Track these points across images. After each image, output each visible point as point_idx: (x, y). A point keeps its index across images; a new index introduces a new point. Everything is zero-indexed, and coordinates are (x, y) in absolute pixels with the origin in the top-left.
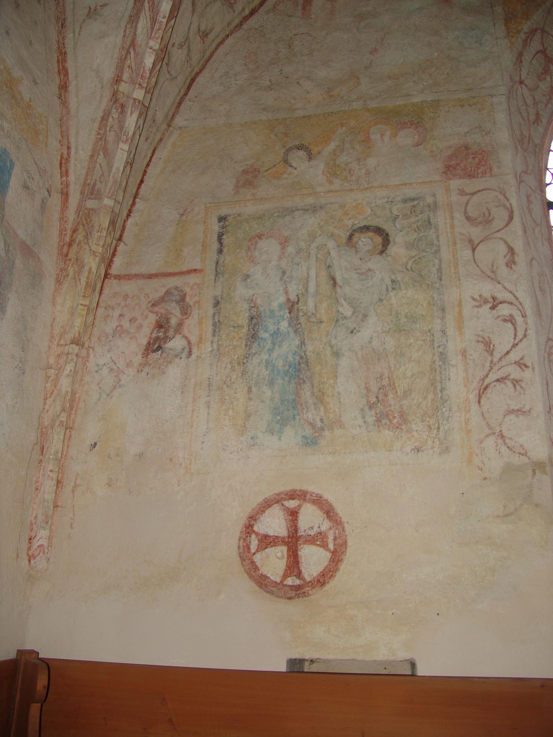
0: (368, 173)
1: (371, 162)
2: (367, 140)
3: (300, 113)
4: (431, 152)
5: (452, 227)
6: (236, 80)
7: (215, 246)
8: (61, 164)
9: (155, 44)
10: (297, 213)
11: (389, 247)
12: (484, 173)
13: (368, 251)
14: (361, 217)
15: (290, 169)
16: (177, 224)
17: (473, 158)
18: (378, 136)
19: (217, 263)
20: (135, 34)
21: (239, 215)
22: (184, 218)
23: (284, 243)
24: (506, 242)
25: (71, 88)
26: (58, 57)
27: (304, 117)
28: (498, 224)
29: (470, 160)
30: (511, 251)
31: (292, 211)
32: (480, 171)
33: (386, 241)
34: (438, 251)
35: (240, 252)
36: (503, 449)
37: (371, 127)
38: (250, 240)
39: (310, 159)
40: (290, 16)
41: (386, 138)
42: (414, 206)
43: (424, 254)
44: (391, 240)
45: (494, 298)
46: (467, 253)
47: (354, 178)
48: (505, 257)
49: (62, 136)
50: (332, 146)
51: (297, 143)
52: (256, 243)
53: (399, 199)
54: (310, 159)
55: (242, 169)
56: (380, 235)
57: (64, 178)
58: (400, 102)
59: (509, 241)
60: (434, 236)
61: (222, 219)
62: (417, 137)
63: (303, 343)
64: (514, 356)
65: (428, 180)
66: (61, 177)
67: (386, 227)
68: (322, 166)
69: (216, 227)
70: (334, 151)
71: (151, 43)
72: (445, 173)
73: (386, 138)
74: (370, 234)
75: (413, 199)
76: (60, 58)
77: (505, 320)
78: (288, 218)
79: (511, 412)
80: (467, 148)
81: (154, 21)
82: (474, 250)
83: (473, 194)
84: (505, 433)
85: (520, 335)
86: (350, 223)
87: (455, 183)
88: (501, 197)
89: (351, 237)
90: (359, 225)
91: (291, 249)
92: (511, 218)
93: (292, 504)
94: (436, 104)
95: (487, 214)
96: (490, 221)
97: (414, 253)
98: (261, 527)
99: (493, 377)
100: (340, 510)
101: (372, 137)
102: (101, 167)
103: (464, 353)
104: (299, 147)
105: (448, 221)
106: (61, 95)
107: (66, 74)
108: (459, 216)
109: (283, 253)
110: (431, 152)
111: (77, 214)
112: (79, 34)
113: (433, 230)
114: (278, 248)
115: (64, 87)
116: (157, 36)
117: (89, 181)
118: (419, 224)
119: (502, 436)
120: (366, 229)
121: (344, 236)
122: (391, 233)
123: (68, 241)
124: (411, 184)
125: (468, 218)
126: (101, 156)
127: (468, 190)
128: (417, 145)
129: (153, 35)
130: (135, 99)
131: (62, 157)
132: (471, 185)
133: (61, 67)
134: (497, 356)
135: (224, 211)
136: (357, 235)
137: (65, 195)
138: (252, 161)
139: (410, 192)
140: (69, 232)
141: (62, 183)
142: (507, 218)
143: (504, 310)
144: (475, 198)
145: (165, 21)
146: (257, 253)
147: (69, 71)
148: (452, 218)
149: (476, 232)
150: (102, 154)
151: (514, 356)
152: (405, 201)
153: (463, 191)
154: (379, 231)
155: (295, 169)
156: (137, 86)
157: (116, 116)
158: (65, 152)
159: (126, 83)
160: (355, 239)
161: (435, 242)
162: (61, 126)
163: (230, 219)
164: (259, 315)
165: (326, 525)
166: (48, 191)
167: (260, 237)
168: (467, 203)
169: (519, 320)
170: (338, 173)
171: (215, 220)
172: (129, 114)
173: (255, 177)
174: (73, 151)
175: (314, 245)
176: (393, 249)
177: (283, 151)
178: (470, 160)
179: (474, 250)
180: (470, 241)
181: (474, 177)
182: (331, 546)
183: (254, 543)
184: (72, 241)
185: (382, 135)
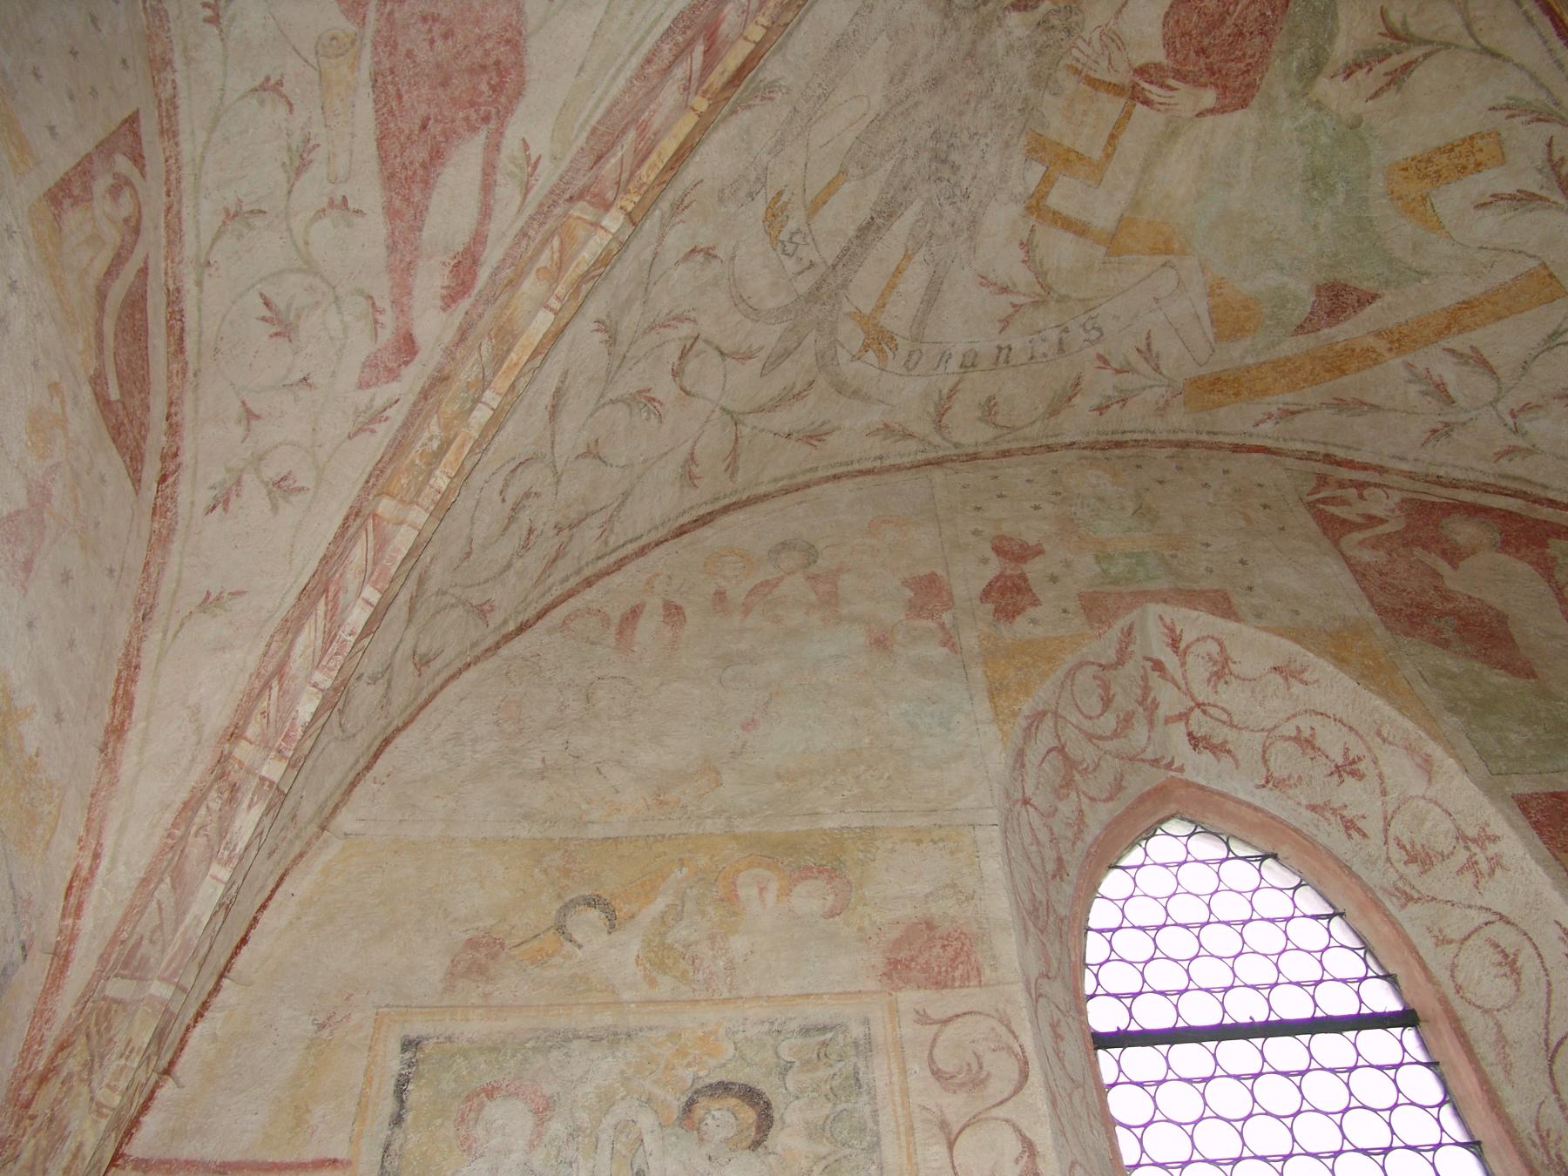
0: (731, 967)
1: (738, 944)
2: (730, 899)
3: (596, 831)
4: (860, 929)
5: (905, 1092)
6: (475, 752)
7: (388, 1106)
8: (70, 887)
9: (325, 680)
10: (576, 1044)
11: (772, 1132)
12: (966, 979)
13: (727, 1140)
14: (712, 1062)
15: (568, 946)
16: (308, 1048)
17: (944, 947)
18: (754, 892)
19: (386, 1149)
20: (288, 654)
21: (449, 1039)
22: (325, 1033)
23: (544, 1110)
24: (1017, 1130)
25: (133, 735)
26: (120, 672)
27: (606, 839)
28: (999, 1086)
29: (937, 950)
30: (1029, 1147)
31: (565, 1038)
32: (957, 974)
33: (766, 1119)
34: (876, 1145)
35: (442, 1125)
37: (739, 871)
38: (468, 1099)
39: (612, 928)
40: (593, 643)
41: (771, 896)
42: (824, 1044)
43: (847, 1151)
44: (776, 1116)
46: (939, 1150)
47: (700, 976)
48: (1017, 1161)
49: (88, 830)
50: (659, 905)
51: (587, 892)
52: (482, 1106)
53: (793, 1026)
54: (612, 928)
55: (467, 936)
56: (753, 1105)
57: (69, 921)
58: (799, 826)
59: (1023, 1125)
60: (868, 1110)
61: (409, 1044)
62: (831, 898)
65: (853, 988)
66: (63, 916)
67: (767, 1086)
68: (636, 947)
69: (394, 1063)
70: (663, 915)
71: (318, 677)
72: (887, 975)
73: (771, 896)
74: (733, 1101)
75: (825, 1029)
76: (124, 674)
78: (555, 1055)
80: (930, 925)
81: (330, 637)
82: (951, 1146)
83: (946, 1022)
86: (688, 1074)
87: (909, 998)
88: (1002, 1030)
89: (690, 1105)
90: (708, 1081)
91: (556, 1127)
92: (1024, 1075)
94: (868, 835)
95: (975, 1067)
96: (983, 1081)
97: (824, 1148)
101: (742, 892)
102: (160, 909)
104: (592, 902)
105: (895, 1079)
106: (106, 744)
107: (129, 705)
108: (917, 1067)
109: (539, 1135)
110: (860, 929)
111: (79, 1008)
112: (175, 636)
113: (865, 1098)
114: (530, 1121)
115: (117, 731)
116: (332, 664)
117: (125, 935)
118: (834, 1083)
120: (723, 1089)
121: (676, 1103)
122: (777, 1101)
123: (41, 1068)
124: (819, 996)
125: (937, 1074)
126: (166, 885)
127: (935, 1012)
128: (832, 914)
129: (324, 663)
130: (263, 779)
131: (75, 874)
132: (942, 1003)
133: (121, 692)
135: (416, 1028)
136: (703, 1102)
137: (61, 958)
138: (489, 922)
139: (817, 1013)
140: (49, 1048)
141: (61, 931)
142: (1016, 1076)
144: (950, 1030)
145: (352, 639)
146: (479, 1131)
147: (137, 702)
148: (904, 1072)
149: (955, 1106)
150: (168, 880)
152: (806, 1031)
153: (925, 1015)
154: (750, 1095)
155: (580, 947)
156: (273, 754)
157: (215, 806)
158: (87, 864)
159: (251, 743)
160: (699, 1111)
161: (870, 1125)
162: (90, 810)
163: (429, 1047)
166: (23, 948)
167: (490, 1092)
168: (935, 1040)
170: (669, 962)
171: (395, 1045)
172: (245, 806)
173: (494, 956)
174: (104, 863)
175: (609, 1121)
176: (779, 1139)
177: (558, 905)
178: (937, 950)
179: (951, 1146)
180: (944, 1125)
181: (945, 986)
184: (50, 1071)
185: (762, 890)
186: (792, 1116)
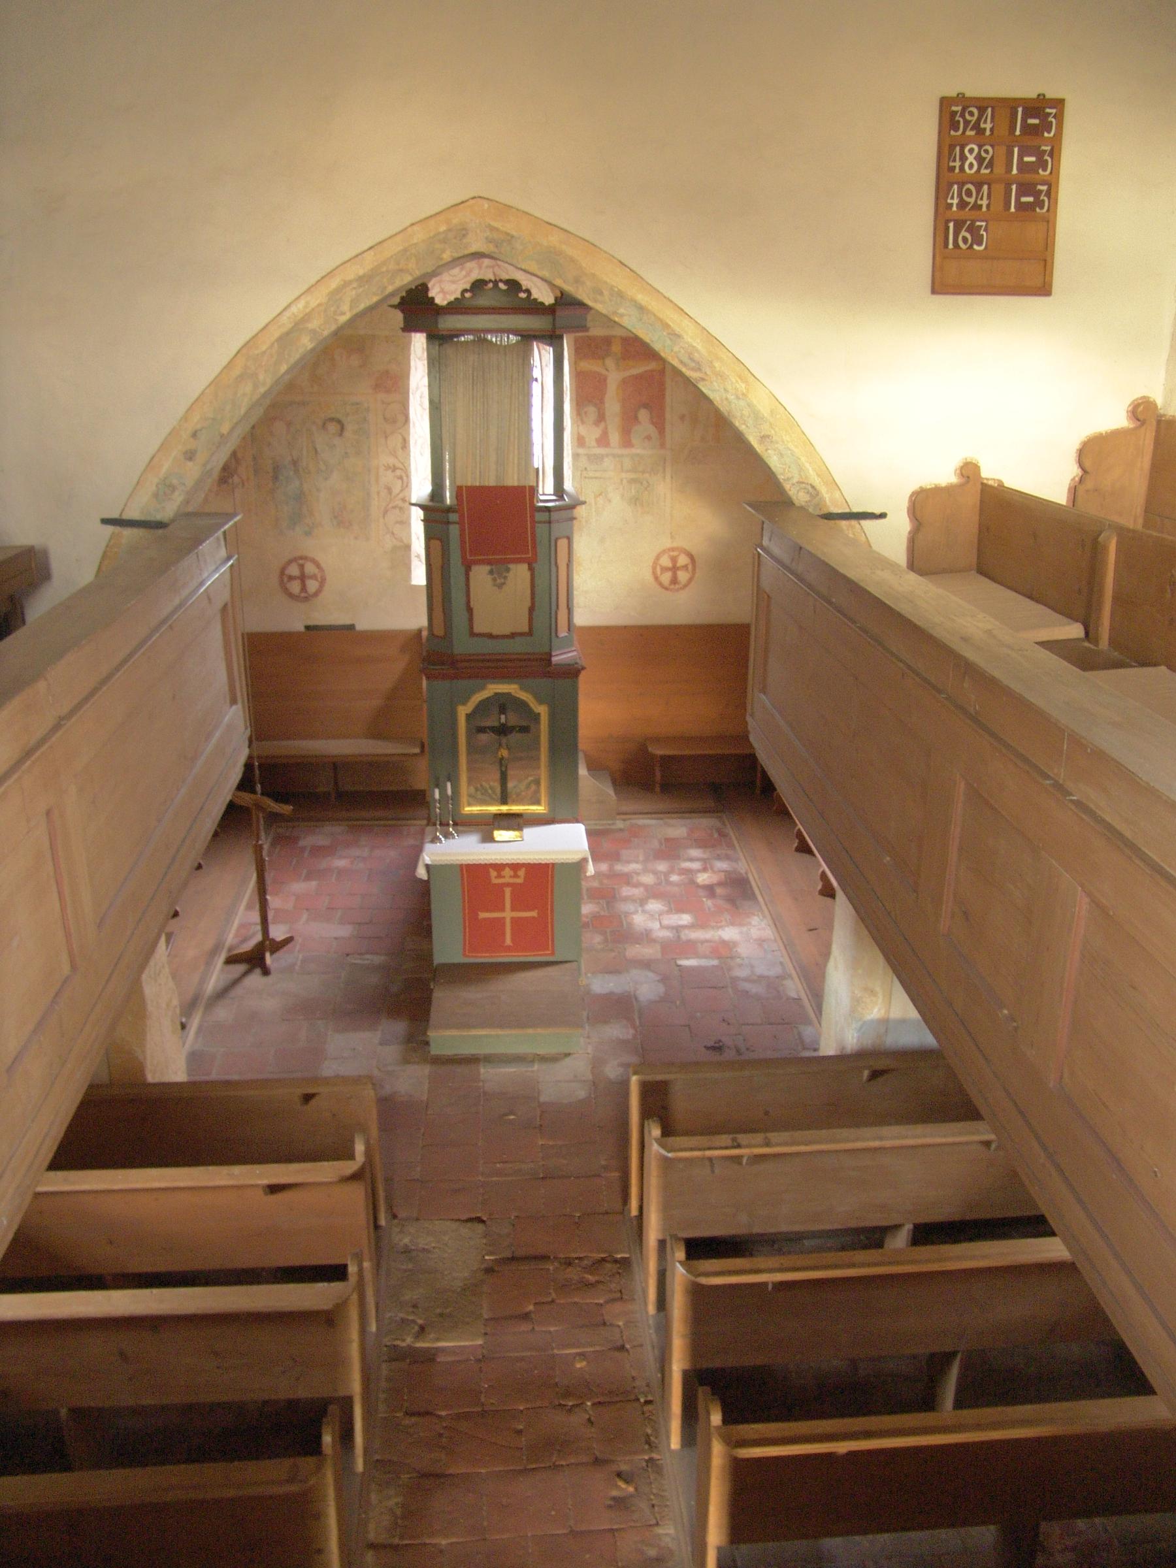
23: (289, 424)
33: (342, 428)
36: (394, 540)
45: (394, 466)
63: (301, 484)
64: (401, 496)
74: (334, 423)
75: (357, 404)
77: (398, 478)
79: (397, 522)
84: (395, 532)
85: (405, 484)
87: (381, 396)
89: (324, 424)
93: (301, 562)
98: (287, 572)
99: (390, 506)
100: (323, 565)
103: (378, 493)
119: (393, 533)
120: (332, 420)
125: (385, 418)
134: (393, 496)
143: (398, 473)
151: (401, 496)
152: (352, 404)
154: (339, 422)
164: (278, 467)
165: (316, 571)
169: (405, 478)
182: (319, 580)
183: (285, 579)
186: (350, 428)
